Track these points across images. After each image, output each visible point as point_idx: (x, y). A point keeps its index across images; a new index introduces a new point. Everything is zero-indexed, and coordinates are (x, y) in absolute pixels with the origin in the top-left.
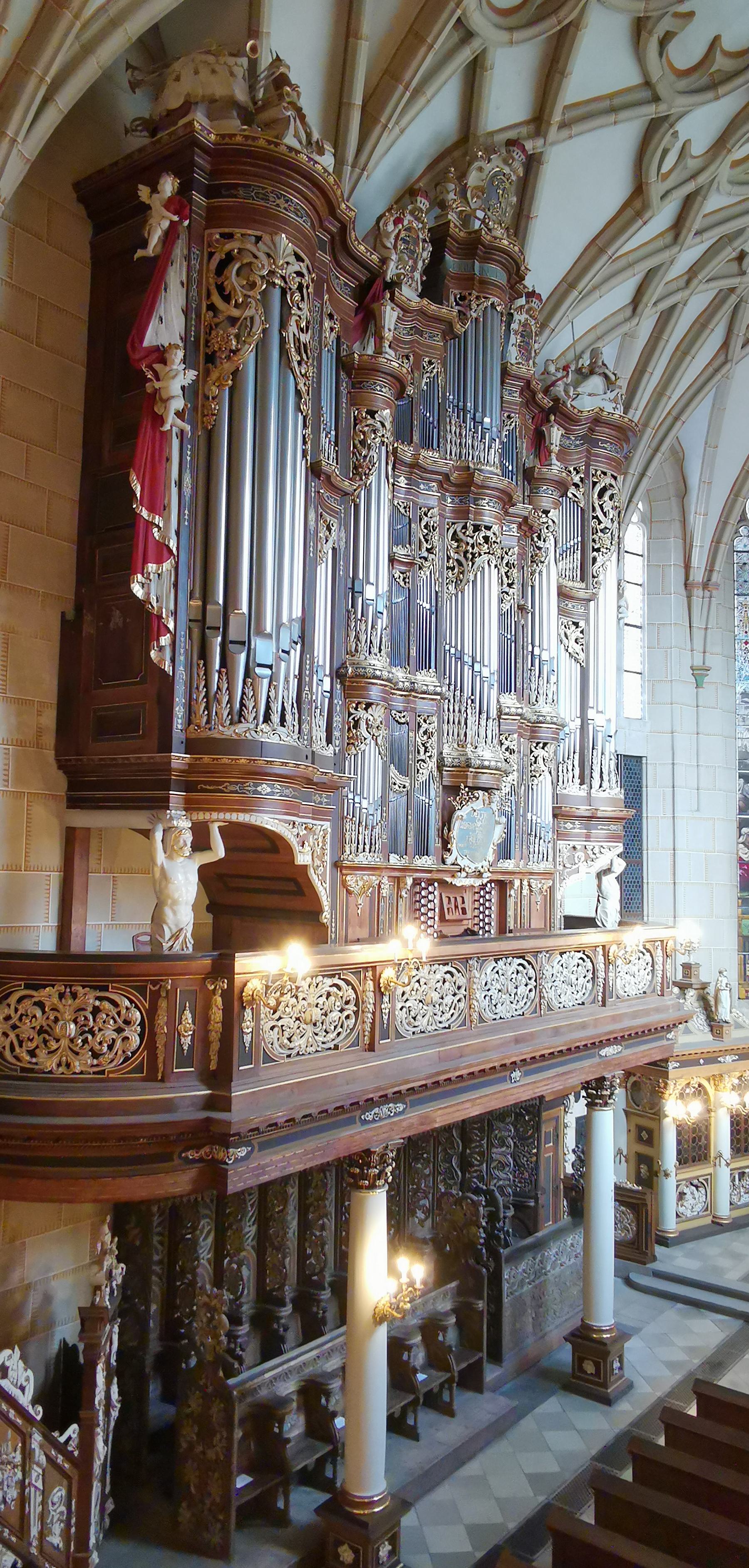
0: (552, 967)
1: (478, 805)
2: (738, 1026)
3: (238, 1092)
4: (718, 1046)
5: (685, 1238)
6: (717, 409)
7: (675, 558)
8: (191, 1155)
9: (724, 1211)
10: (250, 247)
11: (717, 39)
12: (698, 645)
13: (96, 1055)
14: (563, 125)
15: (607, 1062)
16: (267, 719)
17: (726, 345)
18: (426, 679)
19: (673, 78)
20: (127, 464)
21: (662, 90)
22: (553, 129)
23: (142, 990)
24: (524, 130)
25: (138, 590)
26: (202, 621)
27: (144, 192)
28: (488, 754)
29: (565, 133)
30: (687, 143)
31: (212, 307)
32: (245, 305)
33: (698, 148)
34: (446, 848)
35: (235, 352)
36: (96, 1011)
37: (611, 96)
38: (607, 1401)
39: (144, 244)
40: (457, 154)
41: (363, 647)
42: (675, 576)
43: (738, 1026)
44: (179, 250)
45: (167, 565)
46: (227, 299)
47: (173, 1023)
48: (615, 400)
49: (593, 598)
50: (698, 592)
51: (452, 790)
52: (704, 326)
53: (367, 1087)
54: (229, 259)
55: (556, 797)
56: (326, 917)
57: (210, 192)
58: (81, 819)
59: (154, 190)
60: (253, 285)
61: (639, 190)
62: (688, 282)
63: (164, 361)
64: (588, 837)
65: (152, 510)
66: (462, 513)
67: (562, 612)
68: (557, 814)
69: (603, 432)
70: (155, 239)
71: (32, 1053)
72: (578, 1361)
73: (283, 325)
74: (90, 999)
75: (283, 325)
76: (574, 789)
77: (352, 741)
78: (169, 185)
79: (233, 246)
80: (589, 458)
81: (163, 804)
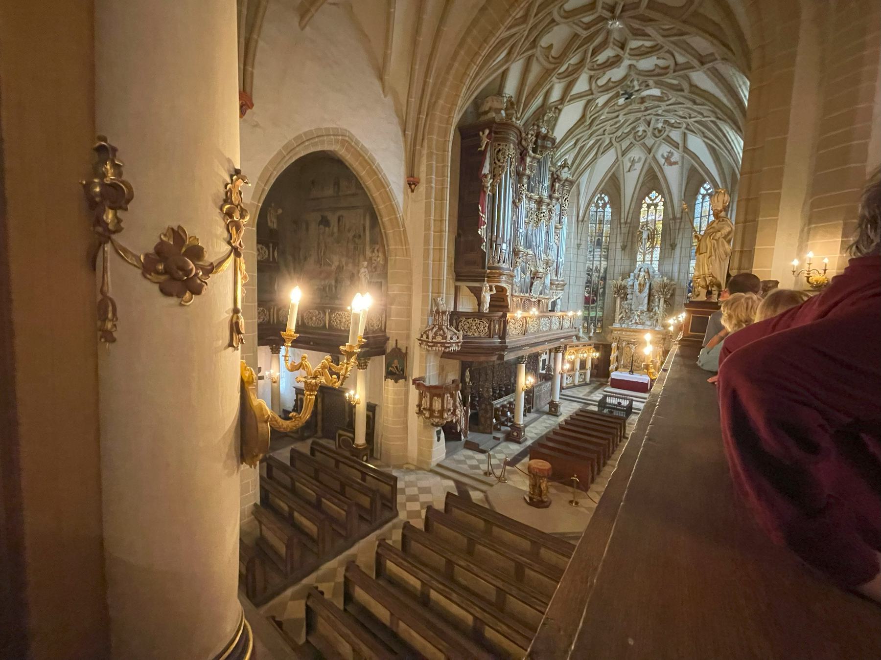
0: (553, 319)
1: (538, 282)
2: (583, 338)
3: (507, 341)
5: (567, 388)
7: (575, 213)
8: (497, 353)
9: (577, 383)
10: (504, 147)
11: (610, 78)
13: (479, 333)
15: (562, 343)
16: (504, 262)
17: (596, 154)
18: (530, 251)
19: (597, 88)
20: (478, 204)
21: (595, 92)
22: (566, 104)
23: (488, 320)
24: (557, 103)
25: (479, 233)
26: (491, 239)
27: (481, 133)
28: (541, 270)
29: (568, 103)
30: (597, 103)
31: (495, 163)
32: (503, 162)
33: (600, 105)
34: (531, 292)
35: (500, 174)
36: (479, 324)
37: (581, 93)
38: (557, 416)
39: (481, 147)
40: (541, 109)
41: (519, 244)
42: (574, 219)
43: (583, 338)
44: (489, 149)
45: (485, 227)
46: (499, 161)
47: (495, 327)
48: (570, 174)
49: (562, 228)
50: (580, 223)
51: (533, 278)
52: (591, 149)
53: (522, 343)
54: (499, 150)
55: (551, 280)
56: (509, 307)
57: (496, 133)
58: (458, 284)
59: (483, 134)
60: (505, 158)
61: (583, 116)
63: (486, 177)
64: (556, 290)
65: (483, 213)
66: (538, 209)
67: (555, 232)
68: (551, 284)
69: (566, 184)
70: (484, 147)
71: (467, 332)
72: (550, 408)
73: (510, 167)
74: (478, 321)
75: (510, 167)
76: (555, 278)
77: (516, 266)
78: (487, 132)
79: (500, 147)
80: (563, 190)
81: (484, 281)
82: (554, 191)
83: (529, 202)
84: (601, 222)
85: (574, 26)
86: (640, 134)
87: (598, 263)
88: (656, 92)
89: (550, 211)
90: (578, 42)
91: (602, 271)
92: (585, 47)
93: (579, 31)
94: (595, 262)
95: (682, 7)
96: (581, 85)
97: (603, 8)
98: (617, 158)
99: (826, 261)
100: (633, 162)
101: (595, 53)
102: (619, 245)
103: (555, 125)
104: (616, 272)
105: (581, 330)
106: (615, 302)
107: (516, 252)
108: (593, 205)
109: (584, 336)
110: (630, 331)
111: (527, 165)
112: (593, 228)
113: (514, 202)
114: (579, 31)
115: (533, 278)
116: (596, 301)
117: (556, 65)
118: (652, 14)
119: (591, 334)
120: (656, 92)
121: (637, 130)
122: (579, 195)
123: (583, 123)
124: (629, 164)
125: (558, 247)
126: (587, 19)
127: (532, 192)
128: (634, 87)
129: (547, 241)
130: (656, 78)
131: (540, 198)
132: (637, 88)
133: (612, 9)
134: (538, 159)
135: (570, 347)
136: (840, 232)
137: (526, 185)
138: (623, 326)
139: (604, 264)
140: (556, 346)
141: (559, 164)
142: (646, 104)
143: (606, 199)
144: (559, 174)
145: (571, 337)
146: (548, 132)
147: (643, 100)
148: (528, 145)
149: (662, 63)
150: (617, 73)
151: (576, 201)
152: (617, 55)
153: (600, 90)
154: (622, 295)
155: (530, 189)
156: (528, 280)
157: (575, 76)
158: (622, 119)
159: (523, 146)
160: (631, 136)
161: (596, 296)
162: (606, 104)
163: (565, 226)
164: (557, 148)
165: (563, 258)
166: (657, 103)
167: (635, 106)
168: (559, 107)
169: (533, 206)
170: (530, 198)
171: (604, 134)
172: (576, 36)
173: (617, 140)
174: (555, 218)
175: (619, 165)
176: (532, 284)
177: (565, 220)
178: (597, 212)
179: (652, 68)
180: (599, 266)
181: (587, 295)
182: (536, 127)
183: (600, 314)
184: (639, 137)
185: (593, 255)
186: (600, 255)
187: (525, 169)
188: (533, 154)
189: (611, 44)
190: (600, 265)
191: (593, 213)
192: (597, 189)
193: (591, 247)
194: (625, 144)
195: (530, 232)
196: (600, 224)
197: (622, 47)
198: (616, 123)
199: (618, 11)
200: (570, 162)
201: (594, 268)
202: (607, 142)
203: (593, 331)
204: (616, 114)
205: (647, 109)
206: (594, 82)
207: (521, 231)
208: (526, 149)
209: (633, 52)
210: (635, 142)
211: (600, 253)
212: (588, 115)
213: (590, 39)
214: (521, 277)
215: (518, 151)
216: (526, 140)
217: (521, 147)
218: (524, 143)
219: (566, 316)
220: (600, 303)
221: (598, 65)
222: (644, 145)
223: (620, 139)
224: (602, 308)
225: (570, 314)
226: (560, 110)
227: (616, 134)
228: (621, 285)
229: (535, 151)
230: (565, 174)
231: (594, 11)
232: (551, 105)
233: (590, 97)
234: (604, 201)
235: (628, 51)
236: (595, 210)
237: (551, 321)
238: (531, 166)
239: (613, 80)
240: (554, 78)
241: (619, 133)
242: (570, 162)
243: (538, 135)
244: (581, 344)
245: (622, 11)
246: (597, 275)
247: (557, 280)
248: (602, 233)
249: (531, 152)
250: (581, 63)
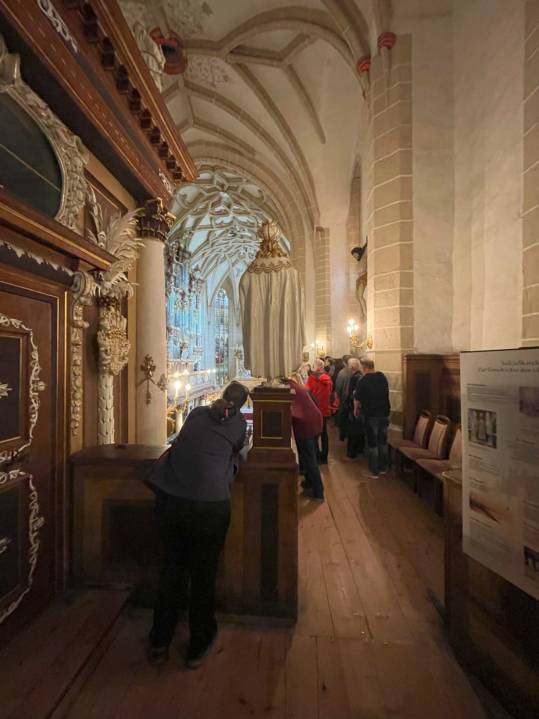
2: (217, 388)
4: (214, 391)
6: (214, 274)
7: (205, 300)
12: (209, 317)
14: (198, 229)
15: (204, 393)
17: (216, 263)
18: (178, 329)
21: (214, 227)
22: (196, 230)
24: (191, 229)
28: (187, 342)
40: (179, 231)
41: (171, 324)
43: (217, 388)
50: (209, 307)
51: (182, 348)
61: (208, 239)
62: (212, 252)
66: (183, 299)
67: (194, 315)
68: (194, 351)
69: (199, 281)
76: (196, 347)
77: (169, 340)
82: (192, 286)
83: (176, 294)
84: (222, 307)
85: (201, 189)
86: (242, 254)
87: (223, 335)
88: (249, 235)
89: (190, 300)
90: (202, 199)
91: (225, 340)
92: (207, 202)
93: (204, 192)
94: (220, 334)
95: (259, 198)
96: (206, 221)
97: (217, 184)
98: (229, 267)
99: (323, 345)
100: (239, 271)
101: (213, 205)
102: (234, 324)
103: (190, 242)
104: (234, 341)
105: (215, 383)
106: (235, 361)
107: (169, 330)
108: (217, 295)
109: (218, 386)
110: (246, 380)
111: (173, 269)
112: (217, 311)
113: (166, 294)
114: (204, 192)
115: (182, 348)
116: (223, 361)
117: (190, 208)
118: (244, 197)
119: (222, 384)
120: (249, 235)
121: (240, 252)
122: (207, 288)
123: (208, 244)
124: (237, 272)
125: (197, 325)
126: (208, 187)
127: (178, 287)
128: (236, 229)
129: (189, 320)
130: (248, 228)
131: (183, 291)
132: (238, 230)
133: (223, 186)
134: (179, 265)
135: (209, 395)
136: (326, 334)
137: (173, 283)
138: (242, 377)
139: (226, 335)
140: (201, 395)
141: (193, 267)
142: (243, 239)
143: (224, 291)
144: (194, 275)
145: (209, 388)
146: (185, 247)
147: (242, 237)
148: (173, 256)
149: (251, 221)
150: (227, 220)
151: (205, 292)
152: (225, 210)
153: (217, 226)
154: (240, 357)
155: (176, 285)
156: (179, 350)
157: (202, 215)
158: (230, 244)
159: (170, 256)
160: (237, 255)
161: (223, 357)
162: (221, 234)
163: (200, 310)
164: (192, 258)
165: (201, 333)
166: (249, 240)
167: (237, 239)
168: (192, 232)
169: (180, 297)
170: (177, 292)
171: (221, 252)
172: (201, 194)
173: (229, 256)
174: (194, 305)
175: (231, 272)
176: (181, 352)
177: (200, 306)
178: (219, 300)
179: (246, 221)
180: (223, 337)
181: (217, 357)
182: (177, 244)
183: (226, 370)
184: (241, 256)
185: (219, 329)
186: (224, 329)
187: (172, 271)
188: (177, 262)
189: (222, 204)
190: (224, 336)
191: (217, 301)
192: (218, 285)
193: (217, 324)
194: (234, 259)
195: (177, 315)
196: (222, 308)
197: (229, 207)
198: (228, 246)
199: (226, 188)
200: (200, 267)
201: (220, 338)
202: (223, 256)
203: (223, 382)
204: (227, 241)
205: (244, 242)
206: (213, 222)
207: (172, 315)
208: (172, 258)
209: (235, 211)
210: (239, 259)
211: (223, 328)
212: (211, 239)
213: (210, 198)
214: (173, 347)
215: (167, 259)
216: (172, 251)
217: (168, 256)
218: (170, 254)
219: (206, 373)
220: (225, 362)
221: (216, 212)
222: (245, 261)
223: (230, 256)
224: (227, 366)
225: (209, 371)
226: (193, 234)
227: (227, 253)
228: (238, 350)
229: (177, 259)
230: (198, 275)
231: (212, 185)
232: (187, 229)
233: (211, 229)
234: (224, 293)
235: (232, 210)
236: (218, 299)
237: (196, 377)
238: (176, 269)
239: (224, 222)
240: (189, 215)
241: (229, 252)
242: (200, 267)
243: (179, 249)
244: (216, 392)
245: (228, 189)
246: (222, 343)
247: (198, 348)
248: (224, 315)
249: (175, 260)
250: (205, 209)
